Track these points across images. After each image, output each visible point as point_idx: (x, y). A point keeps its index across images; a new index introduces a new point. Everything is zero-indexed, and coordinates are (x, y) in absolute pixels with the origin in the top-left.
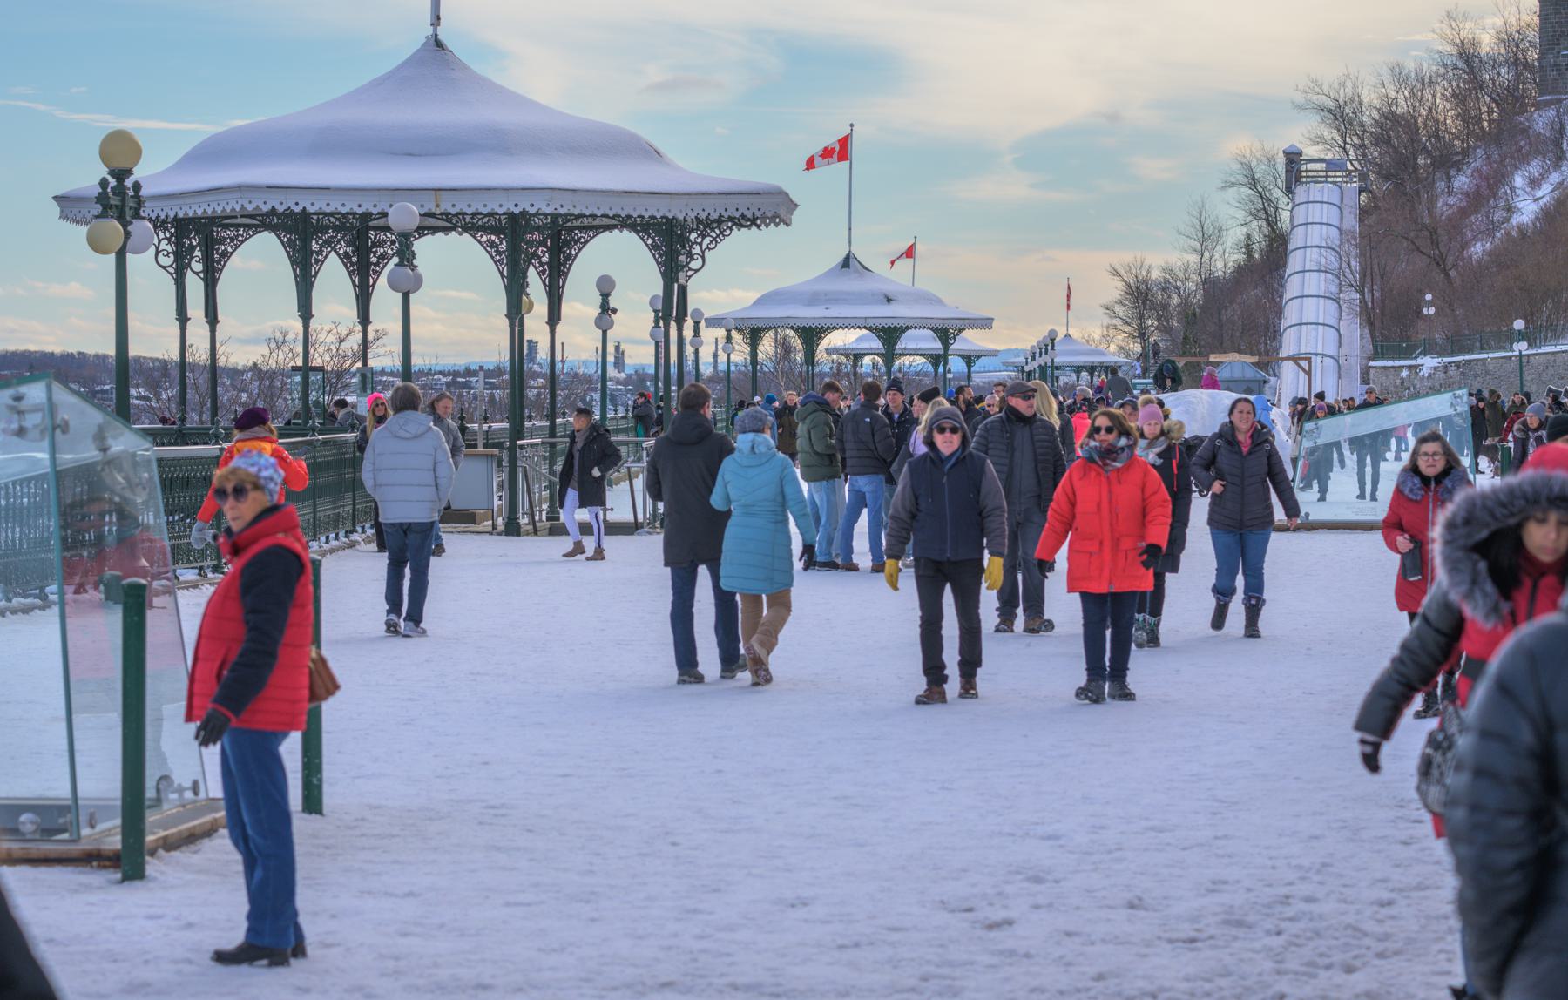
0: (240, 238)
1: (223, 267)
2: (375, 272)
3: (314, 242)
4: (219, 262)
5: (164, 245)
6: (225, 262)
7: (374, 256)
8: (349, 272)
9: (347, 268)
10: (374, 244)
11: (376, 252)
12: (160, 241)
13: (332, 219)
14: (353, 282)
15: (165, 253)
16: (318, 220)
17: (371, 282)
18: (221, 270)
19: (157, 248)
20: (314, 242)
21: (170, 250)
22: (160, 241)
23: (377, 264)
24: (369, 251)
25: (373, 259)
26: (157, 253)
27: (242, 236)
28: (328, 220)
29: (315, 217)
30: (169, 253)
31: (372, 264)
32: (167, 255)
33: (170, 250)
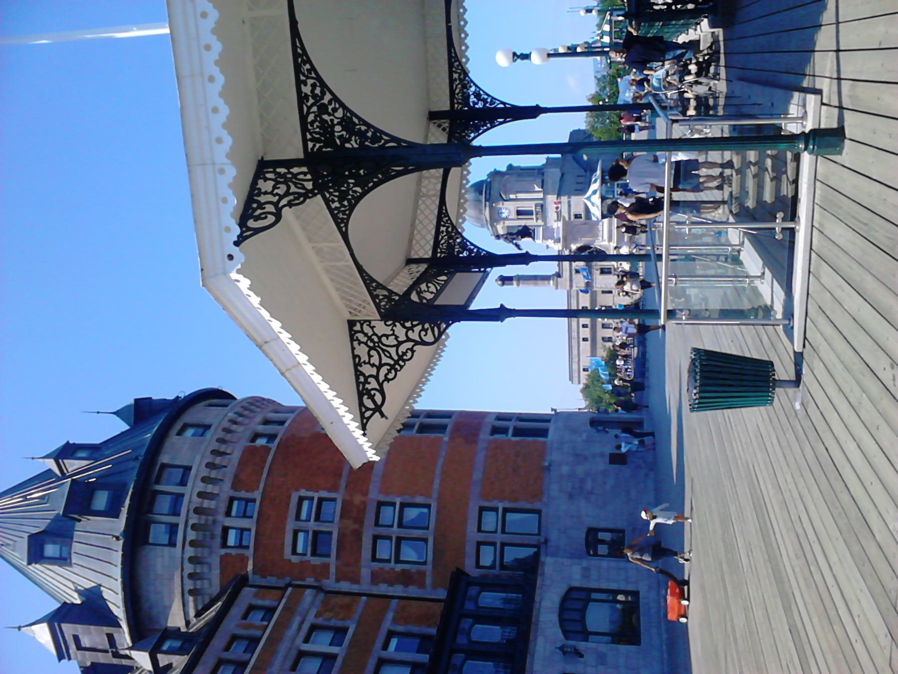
0: (450, 229)
1: (475, 246)
2: (492, 103)
3: (348, 145)
4: (471, 251)
5: (414, 335)
6: (472, 244)
7: (477, 104)
8: (492, 127)
9: (488, 129)
10: (468, 105)
11: (473, 102)
12: (409, 340)
13: (311, 117)
14: (501, 123)
15: (423, 333)
16: (313, 140)
17: (501, 106)
18: (479, 248)
19: (417, 343)
20: (348, 145)
21: (420, 327)
22: (409, 340)
23: (485, 101)
24: (472, 109)
25: (480, 105)
26: (423, 343)
27: (448, 227)
28: (312, 123)
29: (310, 145)
30: (423, 329)
31: (484, 105)
32: (426, 331)
33: (420, 327)
